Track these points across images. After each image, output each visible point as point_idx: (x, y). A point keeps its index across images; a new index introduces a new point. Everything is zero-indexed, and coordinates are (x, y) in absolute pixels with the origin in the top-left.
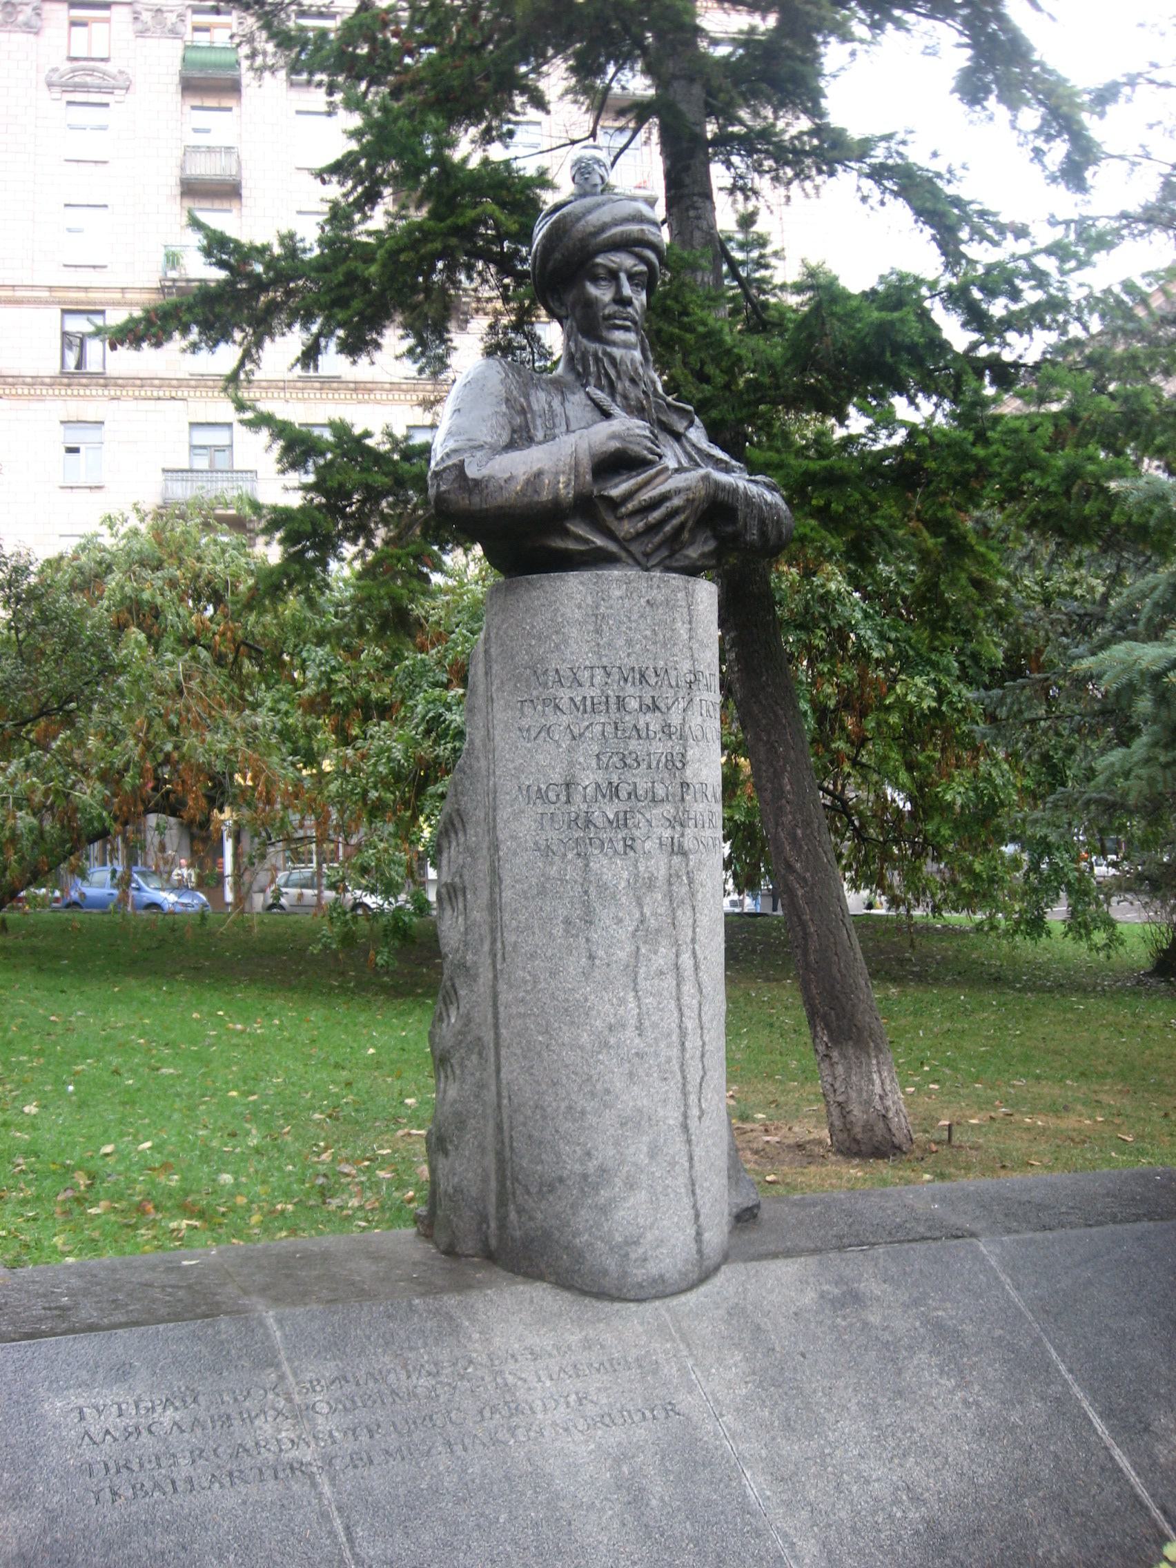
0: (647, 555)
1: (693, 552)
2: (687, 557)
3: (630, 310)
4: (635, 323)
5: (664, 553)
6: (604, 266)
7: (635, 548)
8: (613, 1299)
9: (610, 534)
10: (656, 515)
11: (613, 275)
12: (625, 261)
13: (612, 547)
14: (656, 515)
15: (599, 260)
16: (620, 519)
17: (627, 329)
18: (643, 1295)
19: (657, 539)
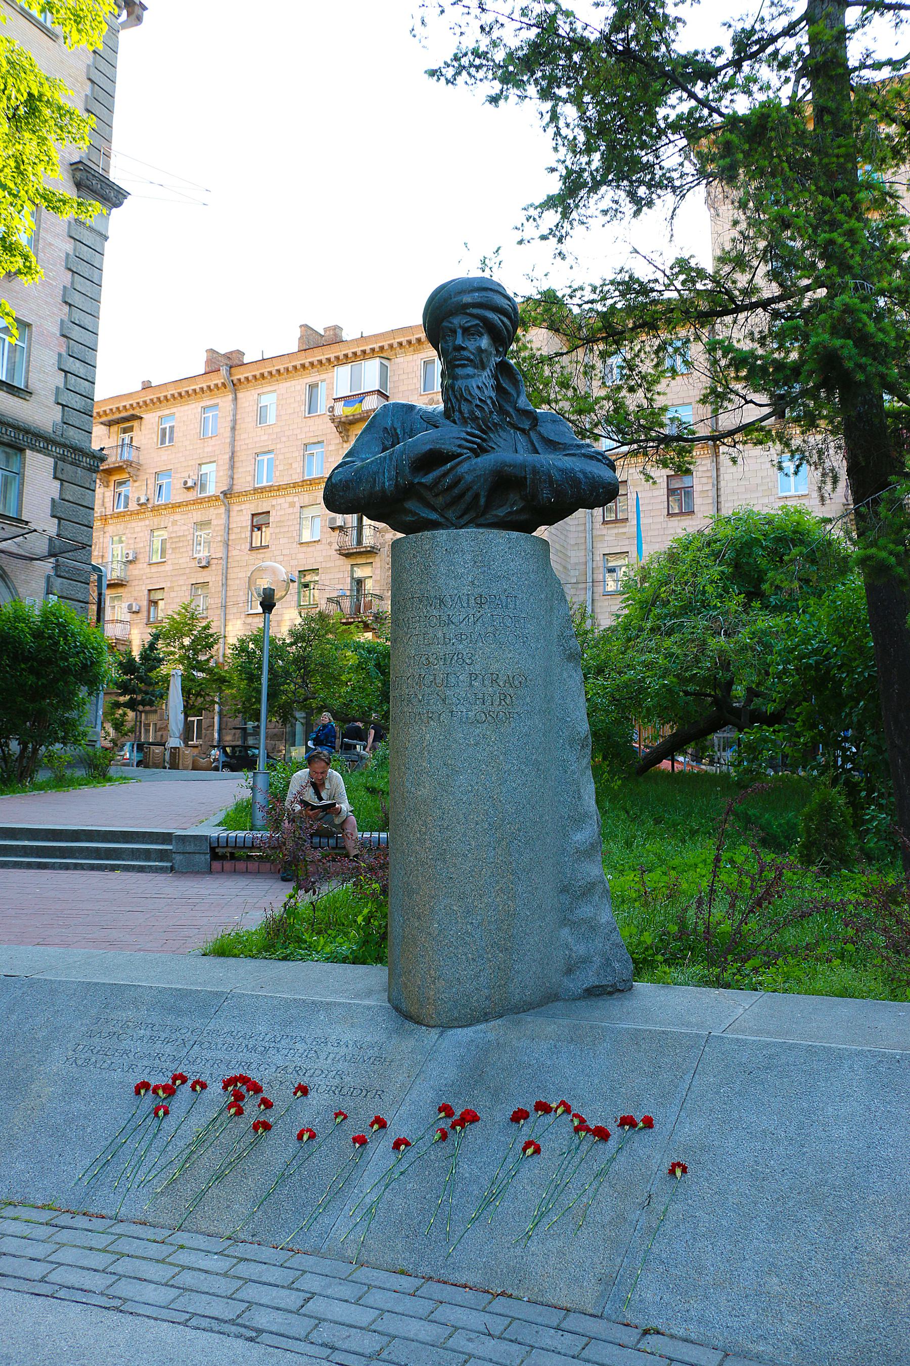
0: (461, 517)
1: (501, 512)
2: (496, 516)
3: (465, 353)
4: (471, 361)
5: (472, 514)
6: (447, 327)
7: (450, 514)
8: (417, 1023)
9: (434, 509)
10: (456, 491)
11: (454, 332)
12: (458, 321)
13: (434, 516)
14: (456, 491)
15: (445, 324)
16: (437, 495)
17: (464, 366)
18: (432, 1023)
19: (462, 506)
